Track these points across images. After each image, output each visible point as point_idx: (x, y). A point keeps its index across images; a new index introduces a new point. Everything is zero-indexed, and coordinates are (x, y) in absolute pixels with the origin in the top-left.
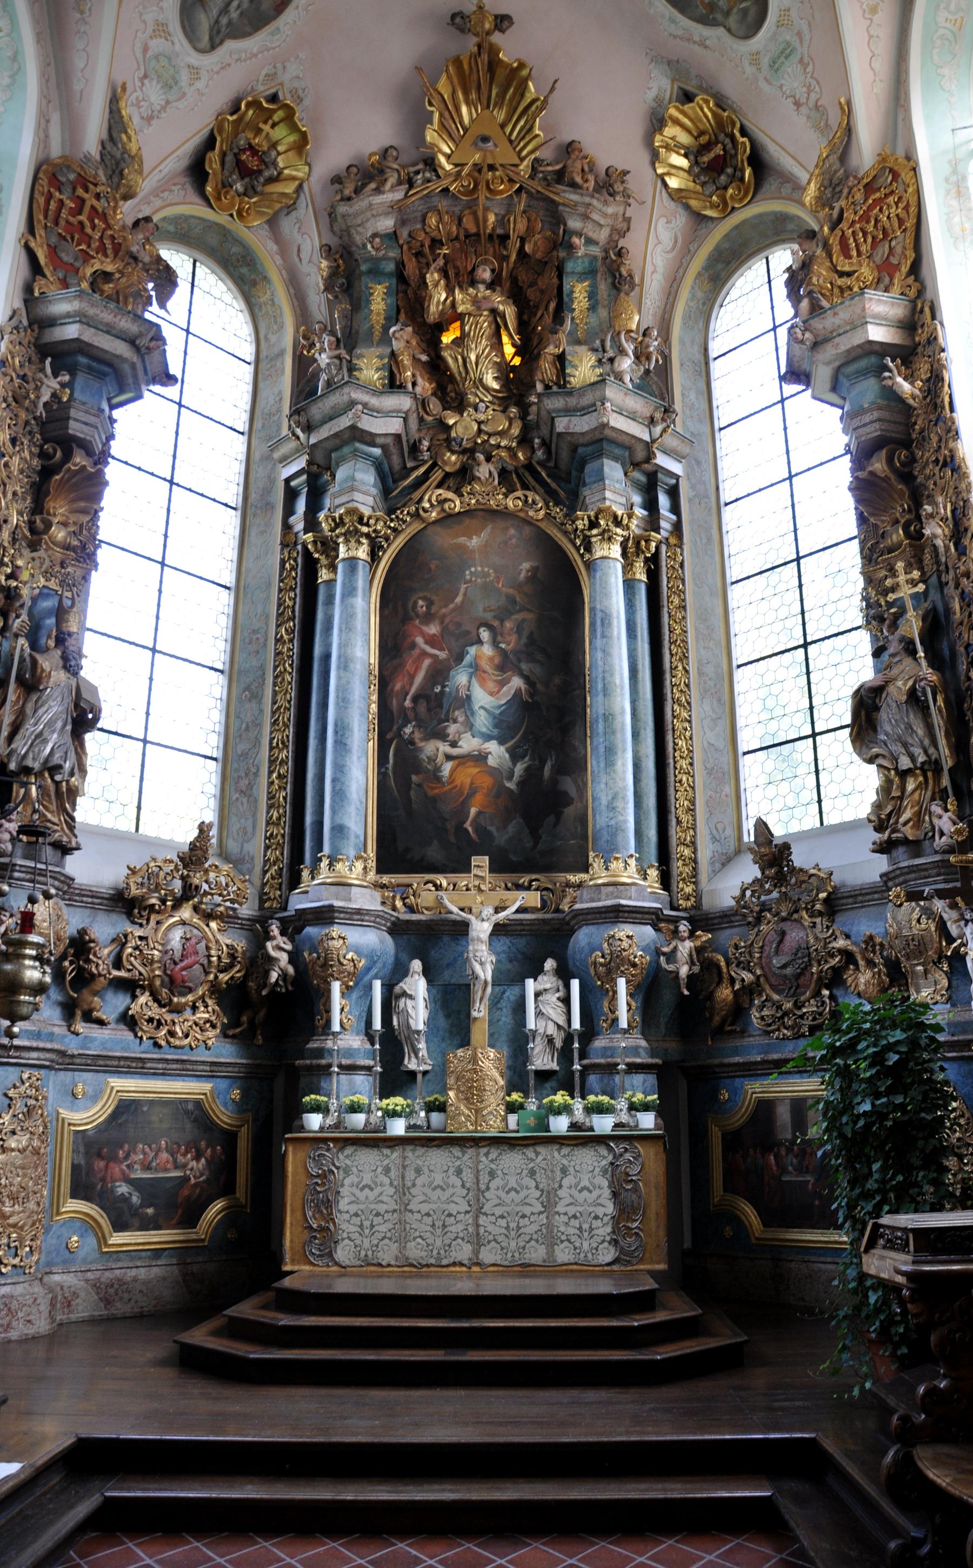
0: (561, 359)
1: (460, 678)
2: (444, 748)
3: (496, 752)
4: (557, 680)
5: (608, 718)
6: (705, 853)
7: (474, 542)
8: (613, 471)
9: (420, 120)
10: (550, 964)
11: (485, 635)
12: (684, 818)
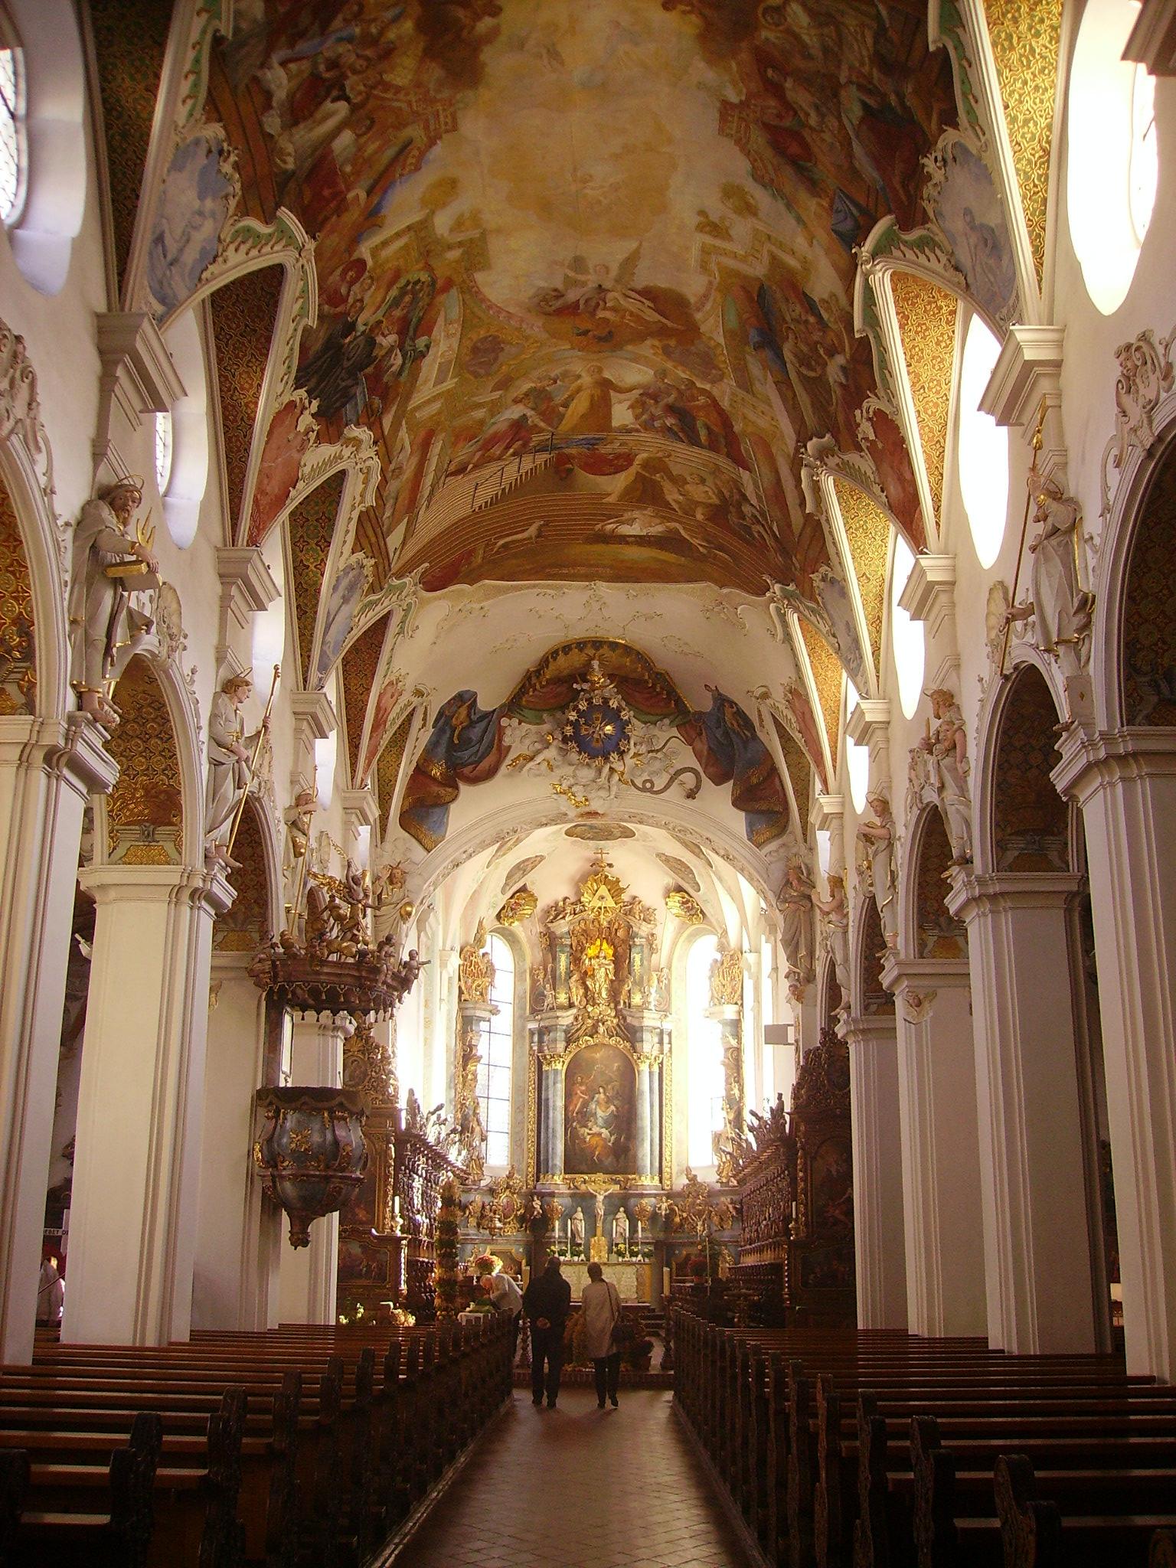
0: (629, 991)
1: (593, 1106)
2: (587, 1131)
3: (605, 1132)
4: (626, 1106)
5: (642, 1128)
6: (675, 1169)
7: (598, 1055)
8: (646, 1036)
9: (579, 894)
10: (622, 1209)
11: (601, 1090)
12: (668, 1158)
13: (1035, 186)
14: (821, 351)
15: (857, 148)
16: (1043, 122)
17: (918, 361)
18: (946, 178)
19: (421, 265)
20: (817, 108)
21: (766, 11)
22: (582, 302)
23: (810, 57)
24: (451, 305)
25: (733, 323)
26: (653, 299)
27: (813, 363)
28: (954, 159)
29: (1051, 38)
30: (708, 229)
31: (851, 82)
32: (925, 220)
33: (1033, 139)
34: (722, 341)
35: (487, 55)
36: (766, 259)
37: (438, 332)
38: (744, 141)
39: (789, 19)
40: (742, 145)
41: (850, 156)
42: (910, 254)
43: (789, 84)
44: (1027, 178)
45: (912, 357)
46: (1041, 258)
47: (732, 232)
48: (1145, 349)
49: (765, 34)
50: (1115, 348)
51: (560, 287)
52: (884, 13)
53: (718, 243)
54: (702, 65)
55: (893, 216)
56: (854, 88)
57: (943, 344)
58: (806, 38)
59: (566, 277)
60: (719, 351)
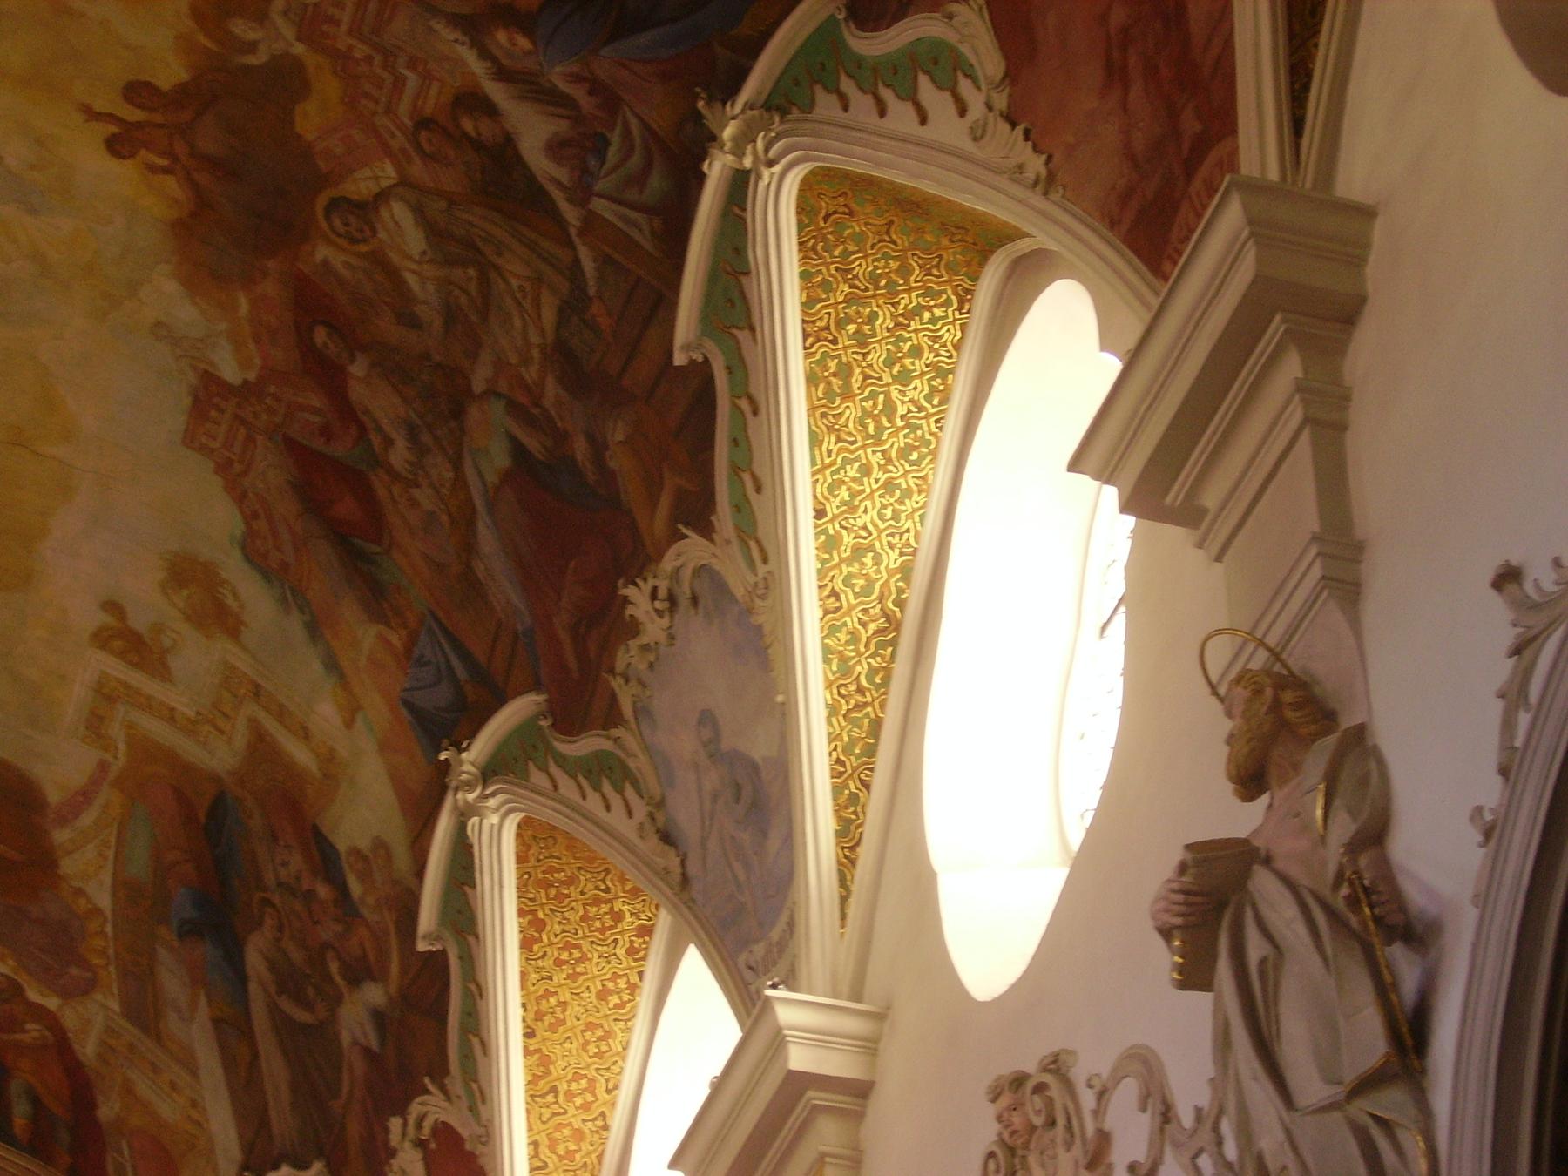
13: (861, 691)
14: (334, 967)
15: (486, 537)
16: (892, 559)
17: (553, 1028)
18: (672, 637)
20: (412, 433)
21: (334, 205)
23: (414, 323)
25: (140, 865)
27: (311, 991)
28: (695, 600)
29: (933, 390)
30: (117, 644)
31: (498, 395)
32: (612, 718)
33: (866, 591)
34: (104, 901)
36: (241, 738)
38: (237, 468)
39: (382, 235)
40: (232, 476)
41: (469, 547)
42: (567, 787)
43: (358, 369)
44: (845, 670)
45: (539, 1016)
46: (852, 849)
47: (175, 663)
48: (1055, 1091)
49: (322, 252)
50: (988, 1080)
52: (588, 265)
53: (137, 679)
54: (172, 287)
55: (541, 698)
56: (497, 409)
57: (614, 1000)
58: (411, 279)
60: (93, 926)
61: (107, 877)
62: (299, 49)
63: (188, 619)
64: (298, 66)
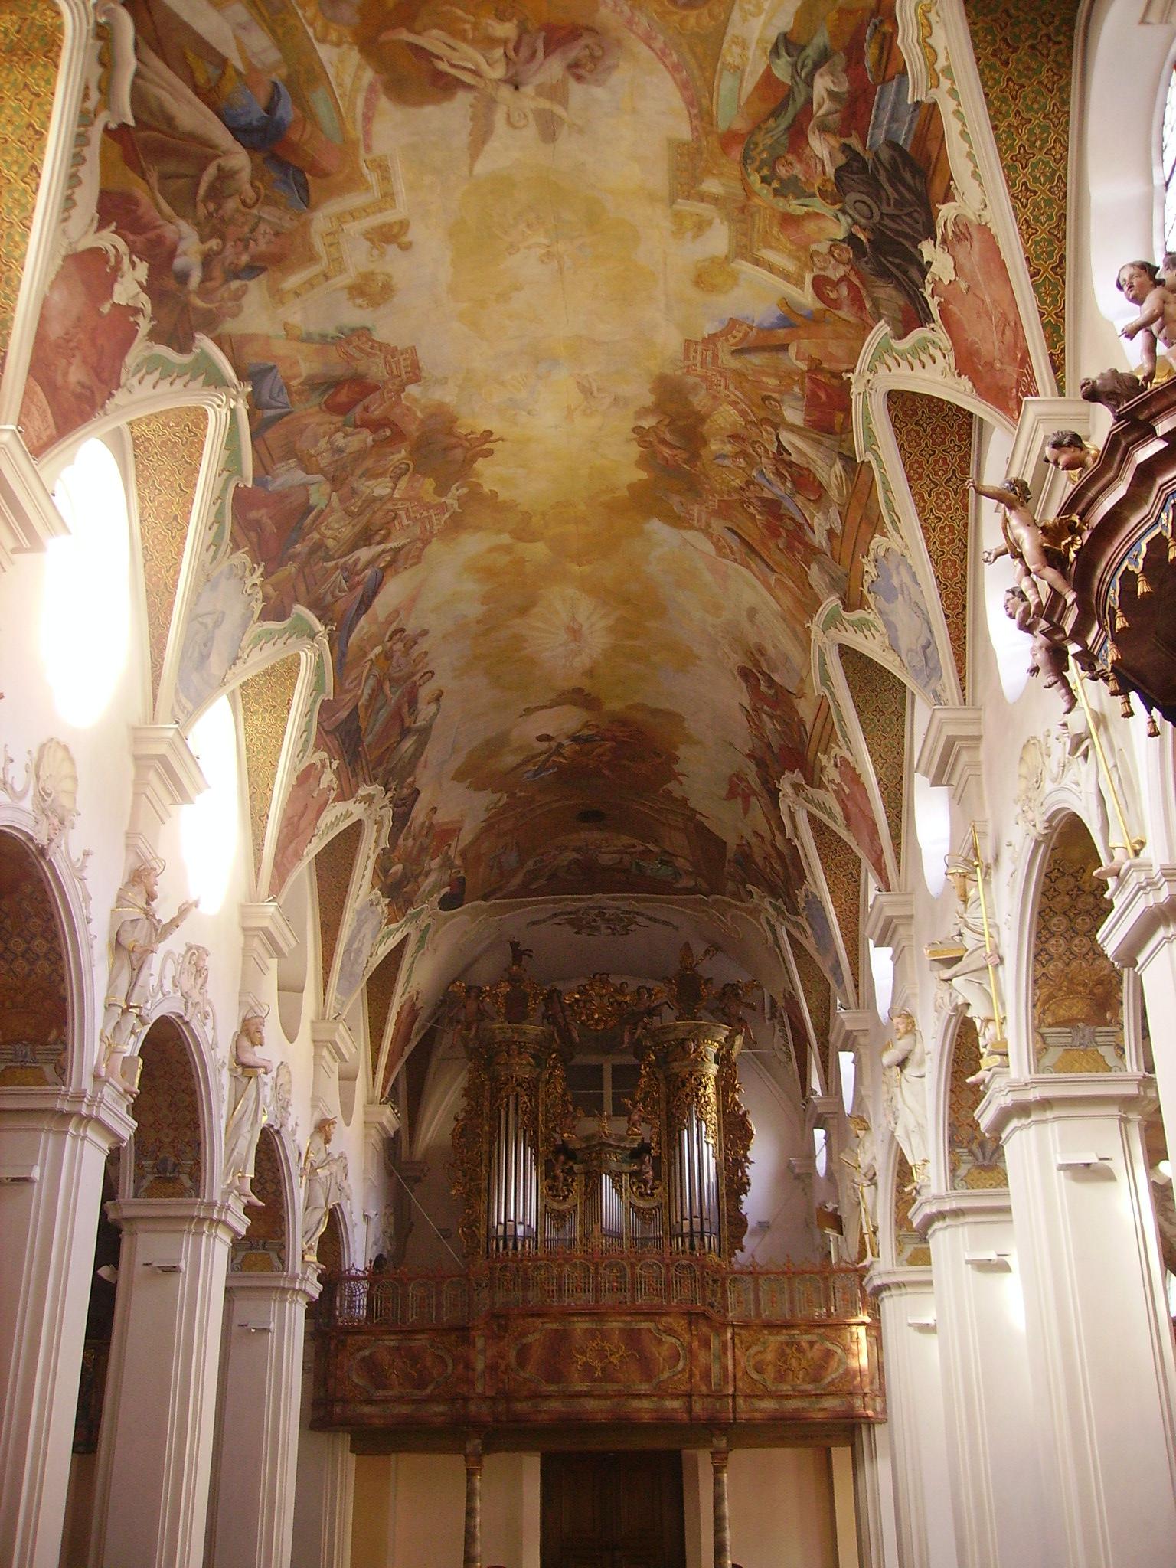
19: (756, 201)
22: (540, 54)
24: (729, 113)
26: (438, 76)
30: (395, 230)
34: (325, 53)
35: (649, 400)
37: (756, 65)
51: (573, 85)
53: (377, 220)
54: (447, 399)
59: (564, 103)
60: (319, 24)
61: (331, 72)
62: (443, 500)
63: (372, 273)
64: (441, 496)
